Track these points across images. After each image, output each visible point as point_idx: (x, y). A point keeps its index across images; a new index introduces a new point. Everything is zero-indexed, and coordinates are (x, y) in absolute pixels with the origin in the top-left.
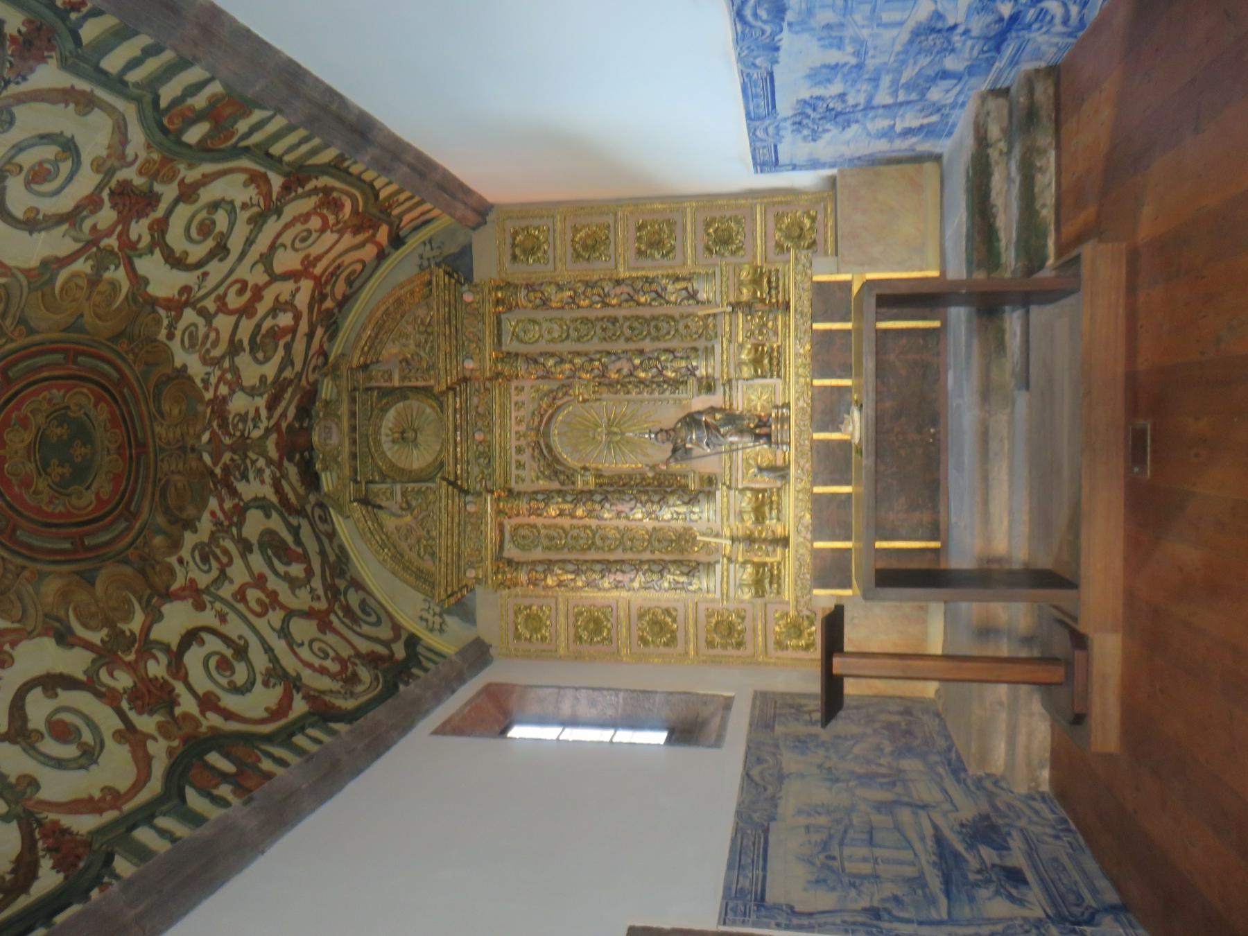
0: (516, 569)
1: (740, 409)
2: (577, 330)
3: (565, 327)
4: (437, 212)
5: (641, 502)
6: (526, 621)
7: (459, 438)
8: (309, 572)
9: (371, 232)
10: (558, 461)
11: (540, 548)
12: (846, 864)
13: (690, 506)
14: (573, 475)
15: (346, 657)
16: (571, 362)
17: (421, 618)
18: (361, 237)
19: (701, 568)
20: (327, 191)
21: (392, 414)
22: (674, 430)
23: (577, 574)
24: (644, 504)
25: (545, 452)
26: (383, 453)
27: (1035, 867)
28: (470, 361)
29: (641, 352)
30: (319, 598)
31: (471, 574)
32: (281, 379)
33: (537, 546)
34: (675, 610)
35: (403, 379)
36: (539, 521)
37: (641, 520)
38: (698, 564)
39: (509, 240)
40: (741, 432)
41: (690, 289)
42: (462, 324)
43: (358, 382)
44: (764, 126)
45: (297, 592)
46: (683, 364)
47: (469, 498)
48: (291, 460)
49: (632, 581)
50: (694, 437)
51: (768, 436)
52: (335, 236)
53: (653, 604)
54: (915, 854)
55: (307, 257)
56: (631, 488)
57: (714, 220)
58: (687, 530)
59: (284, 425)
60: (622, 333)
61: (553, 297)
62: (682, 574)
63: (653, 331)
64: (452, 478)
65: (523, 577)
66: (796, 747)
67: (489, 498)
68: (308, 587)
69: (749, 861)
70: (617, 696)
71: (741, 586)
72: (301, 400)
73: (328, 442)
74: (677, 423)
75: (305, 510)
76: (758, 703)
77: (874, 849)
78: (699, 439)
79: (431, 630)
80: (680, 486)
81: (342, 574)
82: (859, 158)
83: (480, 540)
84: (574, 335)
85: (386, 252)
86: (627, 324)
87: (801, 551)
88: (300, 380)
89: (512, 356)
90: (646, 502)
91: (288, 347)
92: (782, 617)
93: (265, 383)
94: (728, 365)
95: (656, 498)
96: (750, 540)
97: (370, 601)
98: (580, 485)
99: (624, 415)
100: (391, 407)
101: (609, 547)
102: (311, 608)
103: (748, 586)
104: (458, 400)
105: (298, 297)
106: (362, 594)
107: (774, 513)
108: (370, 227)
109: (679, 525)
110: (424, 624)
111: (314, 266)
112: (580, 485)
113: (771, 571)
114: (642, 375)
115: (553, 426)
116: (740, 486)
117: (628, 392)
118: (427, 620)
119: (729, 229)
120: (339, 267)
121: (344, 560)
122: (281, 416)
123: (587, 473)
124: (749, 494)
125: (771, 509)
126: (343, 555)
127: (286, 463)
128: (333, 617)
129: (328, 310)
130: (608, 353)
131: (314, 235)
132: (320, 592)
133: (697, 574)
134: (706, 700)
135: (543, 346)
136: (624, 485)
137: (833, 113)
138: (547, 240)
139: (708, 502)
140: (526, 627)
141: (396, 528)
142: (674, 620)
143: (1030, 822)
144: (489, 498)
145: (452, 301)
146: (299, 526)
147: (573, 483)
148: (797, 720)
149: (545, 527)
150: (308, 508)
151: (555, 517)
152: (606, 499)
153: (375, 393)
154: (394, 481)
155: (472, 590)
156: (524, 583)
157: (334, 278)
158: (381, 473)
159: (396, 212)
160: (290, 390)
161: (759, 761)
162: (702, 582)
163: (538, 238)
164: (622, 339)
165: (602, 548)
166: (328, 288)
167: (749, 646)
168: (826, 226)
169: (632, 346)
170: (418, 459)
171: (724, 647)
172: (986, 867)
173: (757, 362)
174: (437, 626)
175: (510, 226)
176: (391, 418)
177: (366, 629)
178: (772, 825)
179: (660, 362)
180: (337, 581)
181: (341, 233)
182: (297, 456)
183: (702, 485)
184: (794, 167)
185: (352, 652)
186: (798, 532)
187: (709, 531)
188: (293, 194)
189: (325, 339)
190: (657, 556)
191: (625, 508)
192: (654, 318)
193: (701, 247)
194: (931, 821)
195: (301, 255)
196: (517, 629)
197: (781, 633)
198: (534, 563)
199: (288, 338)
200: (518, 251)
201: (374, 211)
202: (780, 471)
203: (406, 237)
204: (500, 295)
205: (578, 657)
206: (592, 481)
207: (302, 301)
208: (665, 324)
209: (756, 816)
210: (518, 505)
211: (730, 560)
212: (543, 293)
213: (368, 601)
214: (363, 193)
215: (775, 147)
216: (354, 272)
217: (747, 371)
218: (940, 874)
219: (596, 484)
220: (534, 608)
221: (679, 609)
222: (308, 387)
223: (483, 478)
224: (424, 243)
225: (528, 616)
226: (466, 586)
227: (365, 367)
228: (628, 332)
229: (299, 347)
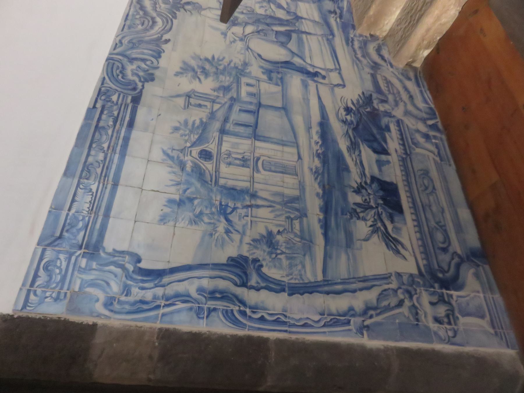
12: (224, 169)
27: (408, 184)
54: (300, 157)
69: (101, 156)
77: (258, 144)
143: (407, 113)
172: (366, 183)
178: (146, 85)
194: (319, 98)
209: (130, 68)
218: (320, 191)
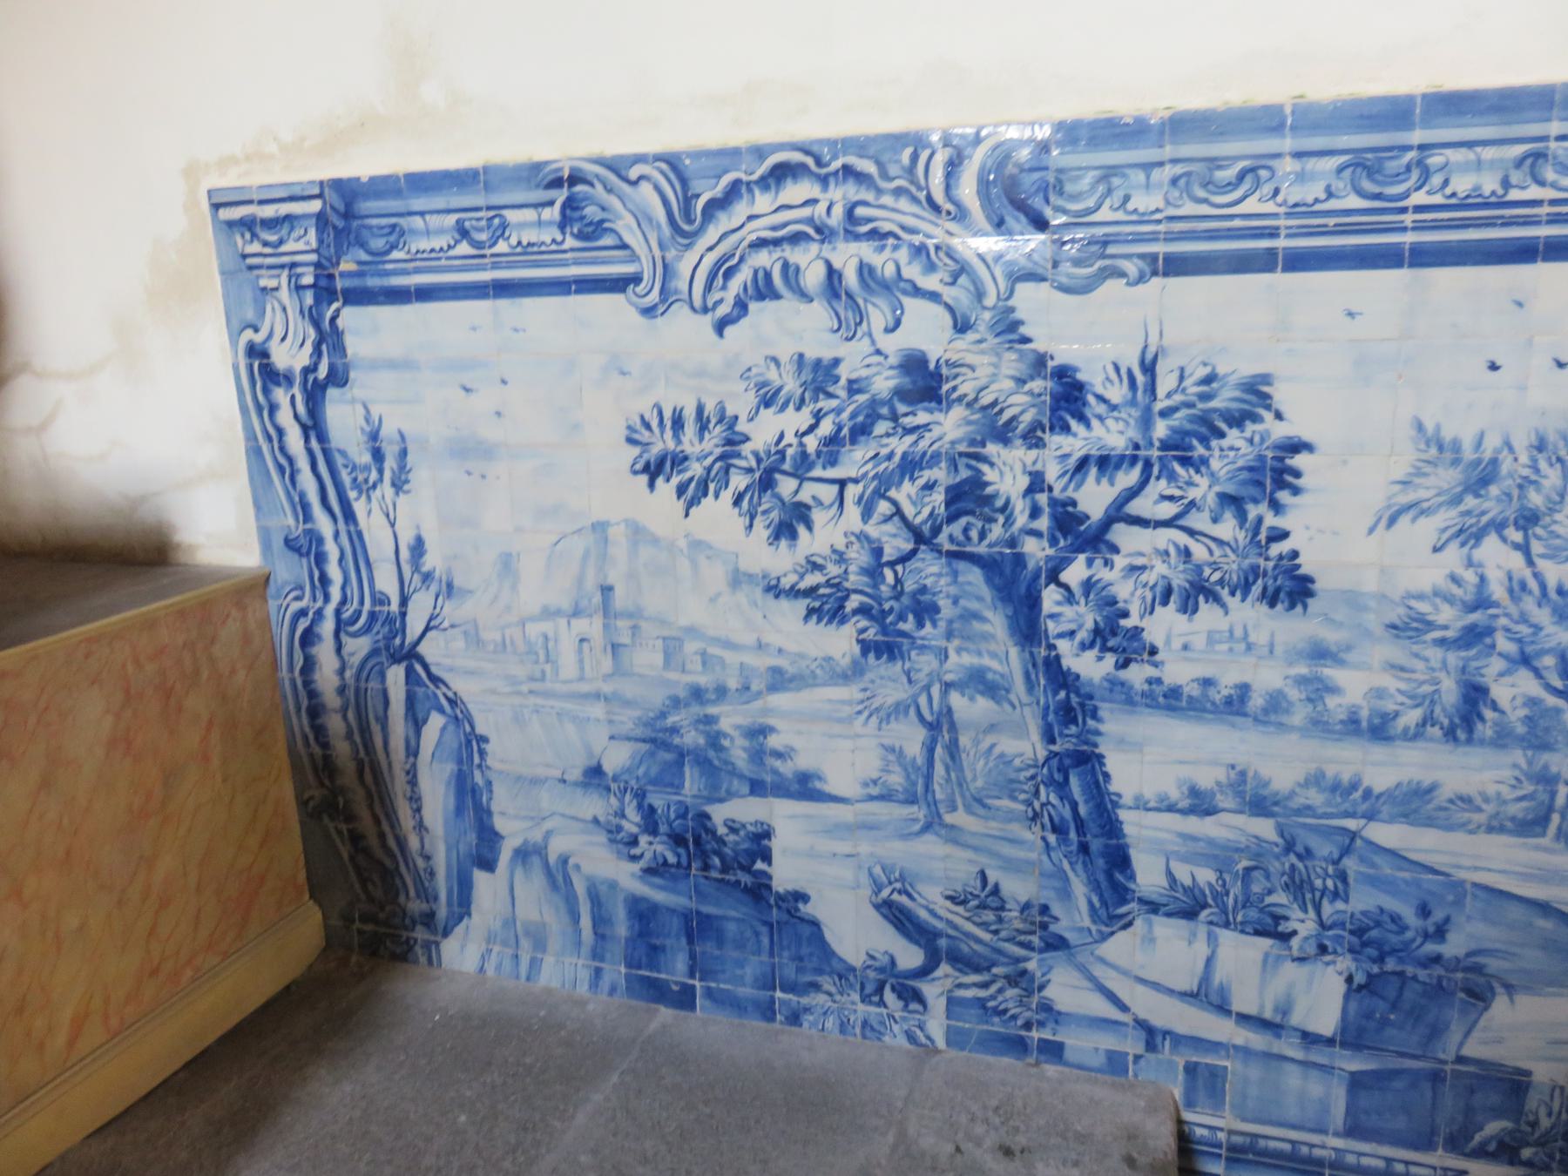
215: (617, 285)
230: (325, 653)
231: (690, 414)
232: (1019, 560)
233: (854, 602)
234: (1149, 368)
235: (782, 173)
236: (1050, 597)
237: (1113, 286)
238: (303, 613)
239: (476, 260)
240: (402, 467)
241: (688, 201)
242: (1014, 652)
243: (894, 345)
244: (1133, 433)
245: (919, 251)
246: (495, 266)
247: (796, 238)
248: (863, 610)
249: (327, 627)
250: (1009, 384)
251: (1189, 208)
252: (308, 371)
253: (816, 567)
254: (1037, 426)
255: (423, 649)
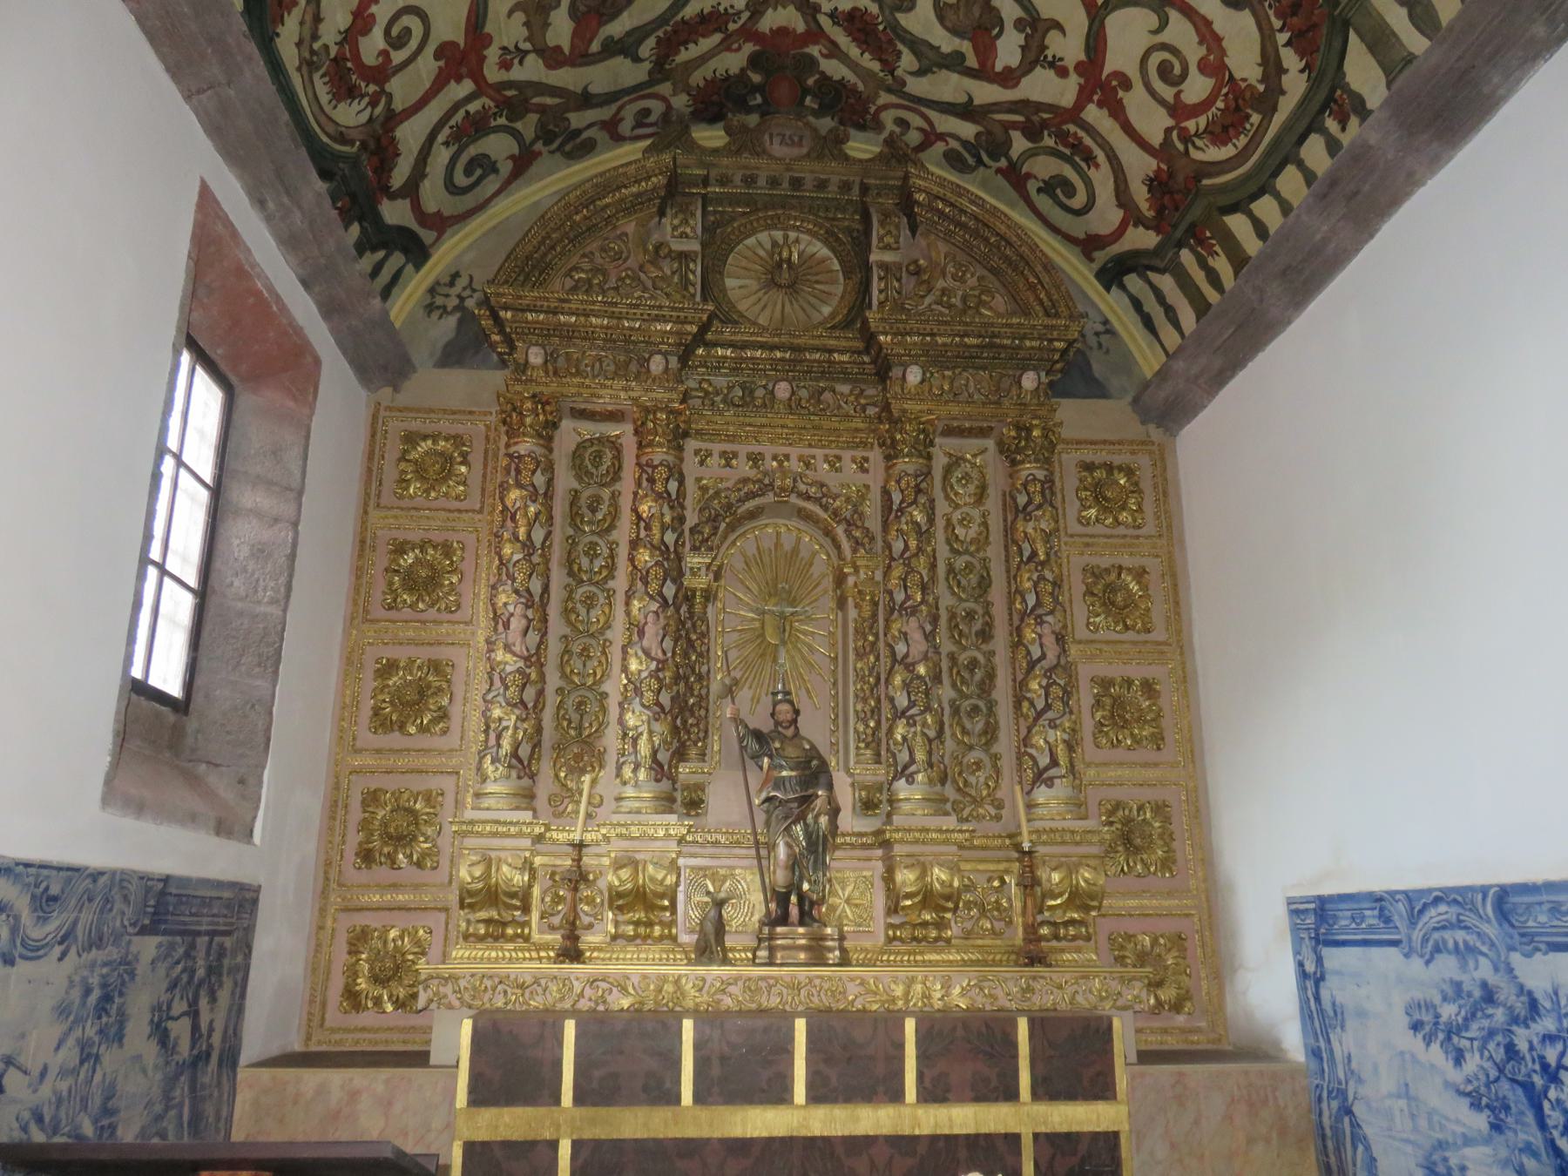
0: (540, 436)
1: (834, 864)
2: (969, 567)
3: (972, 548)
4: (1171, 338)
5: (658, 670)
6: (442, 454)
7: (779, 355)
8: (553, 58)
9: (1150, 214)
10: (732, 528)
11: (576, 485)
13: (649, 761)
14: (711, 549)
15: (388, 88)
16: (920, 549)
17: (455, 276)
18: (1140, 194)
19: (526, 782)
20: (1267, 101)
21: (821, 250)
22: (797, 734)
23: (524, 545)
24: (654, 674)
25: (750, 505)
26: (754, 232)
28: (919, 378)
29: (937, 678)
30: (505, 65)
31: (536, 357)
32: (900, 46)
33: (579, 478)
34: (444, 732)
35: (884, 266)
36: (626, 485)
37: (625, 669)
38: (532, 776)
39: (1117, 460)
40: (794, 864)
41: (1052, 772)
42: (984, 368)
43: (879, 195)
44: (1471, 920)
45: (520, 17)
46: (920, 756)
47: (674, 362)
48: (754, 61)
49: (507, 648)
50: (784, 773)
51: (783, 919)
52: (1156, 139)
53: (459, 690)
55: (1126, 84)
56: (686, 655)
57: (1167, 820)
58: (599, 760)
59: (814, 50)
60: (965, 649)
61: (1031, 524)
62: (516, 746)
63: (966, 705)
64: (709, 336)
65: (526, 446)
66: (88, 991)
67: (675, 396)
68: (527, 46)
70: (273, 601)
71: (488, 862)
72: (854, 91)
73: (776, 140)
74: (809, 742)
75: (666, 79)
76: (226, 894)
78: (779, 784)
79: (432, 291)
80: (683, 745)
81: (546, 136)
82: (1349, 1112)
83: (594, 377)
84: (960, 562)
85: (1098, 255)
86: (981, 658)
87: (553, 988)
88: (889, 90)
89: (923, 449)
90: (659, 680)
91: (954, 62)
92: (418, 943)
93: (899, 9)
94: (916, 842)
95: (665, 699)
96: (578, 878)
97: (492, 184)
98: (693, 560)
99: (811, 649)
100: (833, 250)
101: (573, 610)
102: (487, 40)
103: (487, 874)
104: (845, 358)
105: (1051, 73)
106: (506, 168)
107: (630, 930)
108: (1160, 211)
109: (611, 740)
110: (447, 279)
111: (1100, 104)
112: (693, 560)
113: (514, 922)
114: (898, 680)
115: (794, 523)
116: (681, 862)
117: (860, 655)
118: (452, 284)
119: (1149, 847)
120: (1089, 158)
121: (568, 148)
122: (834, 44)
123: (711, 576)
124: (671, 879)
125: (637, 924)
126: (578, 147)
127: (749, 48)
128: (467, 87)
129: (1008, 143)
130: (935, 620)
131: (1167, 93)
132: (517, 73)
133: (514, 774)
134: (248, 785)
135: (942, 507)
136: (691, 643)
137: (1538, 1080)
138: (1117, 522)
139: (656, 798)
140: (427, 453)
141: (626, 235)
142: (423, 729)
144: (675, 396)
145: (1022, 354)
146: (637, 59)
147: (695, 549)
148: (173, 986)
149: (615, 496)
150: (665, 88)
151: (635, 510)
152: (665, 603)
153: (857, 226)
154: (704, 245)
155: (503, 364)
156: (512, 450)
157: (1067, 151)
158: (717, 224)
159: (1186, 256)
160: (875, 66)
161: (45, 902)
162: (498, 784)
163: (1124, 508)
164: (953, 648)
165: (570, 598)
166: (1049, 141)
167: (364, 876)
168: (1165, 1031)
169: (945, 665)
170: (739, 285)
171: (365, 825)
173: (928, 898)
174: (439, 301)
175: (1143, 462)
176: (812, 249)
177: (441, 156)
179: (922, 713)
180: (533, 118)
181: (1163, 152)
182: (756, 78)
183: (686, 787)
184: (1311, 980)
185: (398, 105)
186: (593, 982)
187: (597, 800)
188: (1277, 24)
189: (954, 144)
190: (552, 700)
191: (651, 639)
192: (991, 705)
193: (1117, 794)
195: (1133, 73)
196: (425, 438)
197: (385, 942)
198: (550, 468)
199: (972, 61)
200: (1097, 474)
201: (1196, 213)
202: (711, 945)
203: (1123, 287)
204: (1035, 433)
205: (363, 545)
206: (701, 582)
207: (1042, 87)
208: (980, 726)
210: (660, 445)
211: (539, 839)
212: (1039, 507)
213: (492, 177)
214: (1247, 177)
215: (1395, 943)
216: (1070, 191)
217: (906, 878)
219: (694, 591)
220: (463, 469)
221: (444, 739)
222: (873, 109)
223: (707, 393)
224: (1106, 322)
225: (447, 459)
226: (512, 348)
227: (907, 204)
228: (963, 658)
229: (949, 86)
230: (1324, 1105)
231: (1422, 1003)
232: (1533, 1084)
233: (1484, 1101)
234: (1556, 993)
235: (1437, 900)
236: (1546, 1105)
237: (1538, 955)
238: (1317, 1086)
239: (1356, 931)
240: (1343, 1020)
241: (1412, 909)
242: (1539, 1134)
243: (1478, 975)
244: (1557, 1024)
245: (1479, 934)
246: (1363, 933)
247: (1444, 928)
248: (1488, 1106)
249: (1325, 1094)
250: (1514, 997)
251: (1556, 923)
252: (1315, 973)
253: (1469, 1081)
254: (1526, 1019)
255: (1355, 1109)
